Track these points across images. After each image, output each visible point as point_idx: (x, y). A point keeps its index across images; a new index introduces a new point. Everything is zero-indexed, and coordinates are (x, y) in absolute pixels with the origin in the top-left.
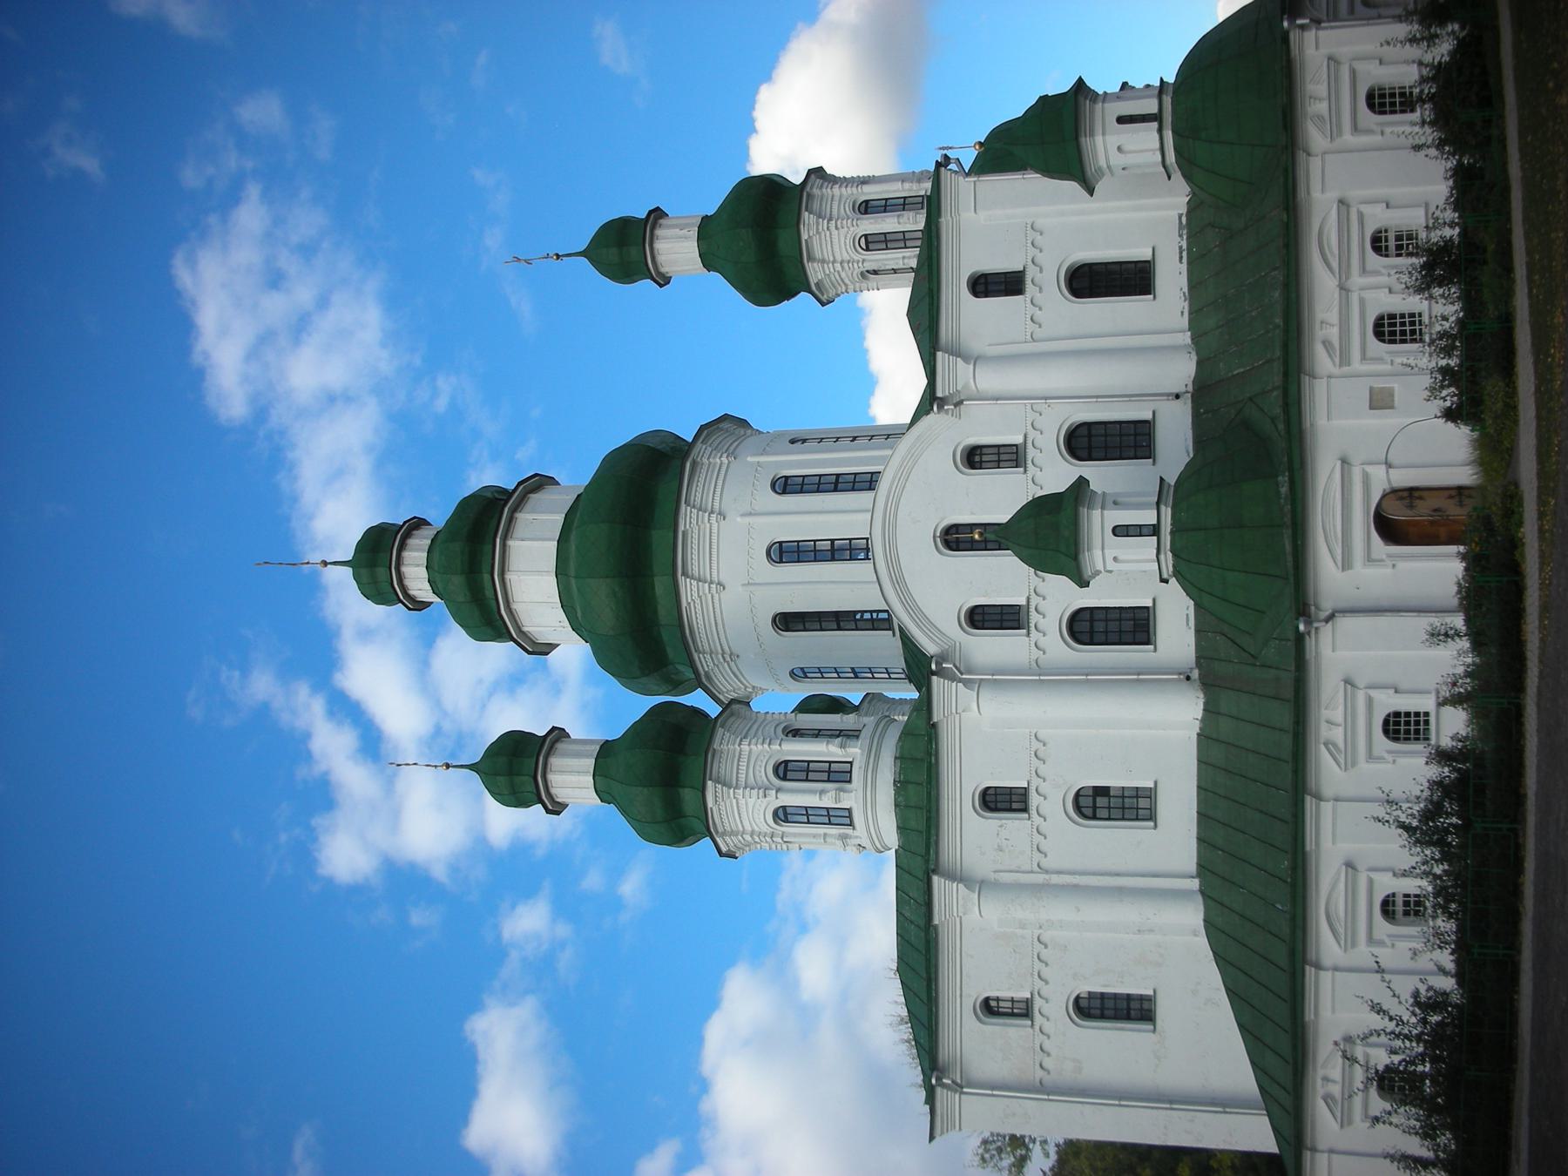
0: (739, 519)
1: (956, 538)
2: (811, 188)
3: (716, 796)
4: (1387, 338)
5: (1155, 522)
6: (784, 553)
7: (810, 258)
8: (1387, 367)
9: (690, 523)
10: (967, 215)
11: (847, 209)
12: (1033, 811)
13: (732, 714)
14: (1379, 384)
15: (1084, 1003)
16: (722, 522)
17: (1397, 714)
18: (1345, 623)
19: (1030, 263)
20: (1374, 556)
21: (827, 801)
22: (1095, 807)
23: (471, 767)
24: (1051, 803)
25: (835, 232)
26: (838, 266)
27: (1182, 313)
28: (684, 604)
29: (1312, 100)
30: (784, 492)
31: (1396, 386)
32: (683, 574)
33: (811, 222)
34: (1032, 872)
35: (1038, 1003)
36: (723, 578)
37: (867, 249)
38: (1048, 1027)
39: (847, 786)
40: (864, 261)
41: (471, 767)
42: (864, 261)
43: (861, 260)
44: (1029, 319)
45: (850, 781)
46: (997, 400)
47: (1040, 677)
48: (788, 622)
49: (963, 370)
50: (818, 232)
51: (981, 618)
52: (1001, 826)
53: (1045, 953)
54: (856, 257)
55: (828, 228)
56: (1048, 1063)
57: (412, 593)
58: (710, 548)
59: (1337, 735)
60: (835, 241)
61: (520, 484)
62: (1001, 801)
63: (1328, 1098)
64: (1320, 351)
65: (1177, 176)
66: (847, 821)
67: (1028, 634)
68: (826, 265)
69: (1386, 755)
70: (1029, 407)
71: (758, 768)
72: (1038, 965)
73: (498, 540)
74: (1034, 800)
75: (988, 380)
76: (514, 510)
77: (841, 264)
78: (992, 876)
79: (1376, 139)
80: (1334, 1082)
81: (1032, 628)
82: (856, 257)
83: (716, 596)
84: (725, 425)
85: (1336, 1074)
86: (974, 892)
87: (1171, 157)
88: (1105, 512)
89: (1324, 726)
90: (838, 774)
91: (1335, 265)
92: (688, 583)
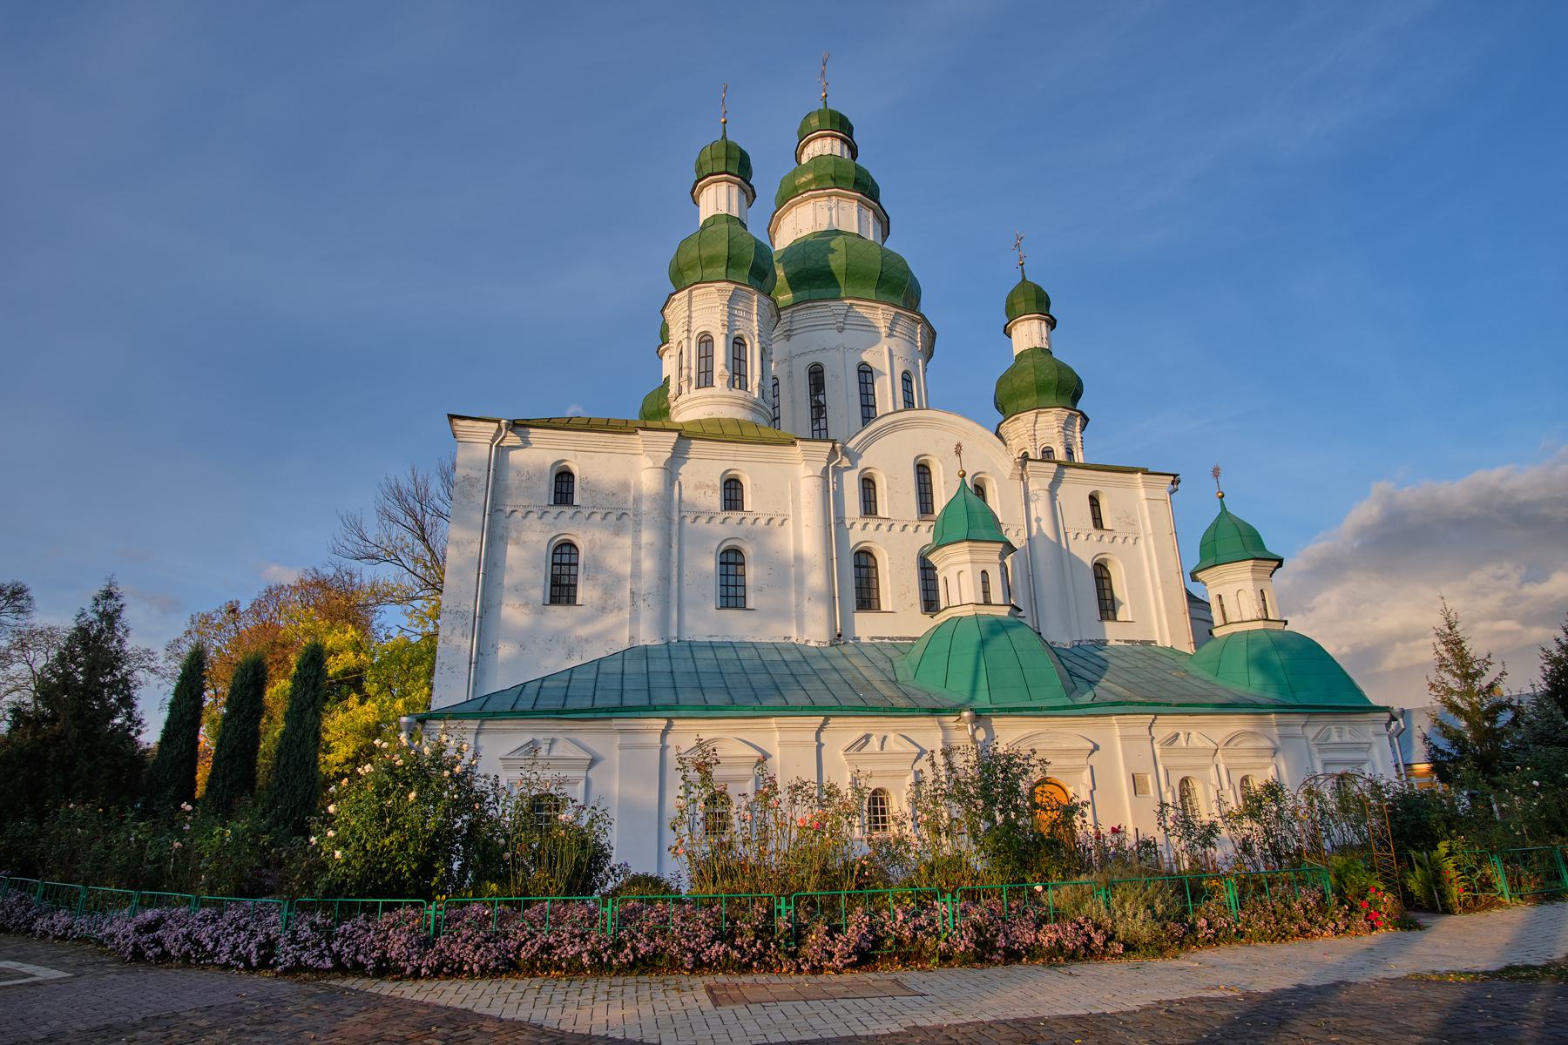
5: (993, 603)
7: (1037, 413)
12: (726, 514)
13: (772, 316)
15: (566, 549)
22: (727, 563)
23: (724, 137)
29: (1339, 730)
30: (903, 379)
34: (680, 512)
35: (569, 511)
36: (845, 332)
37: (1043, 452)
38: (549, 518)
41: (724, 137)
46: (1026, 505)
47: (834, 524)
51: (868, 484)
53: (613, 517)
56: (518, 515)
57: (811, 144)
61: (888, 218)
62: (732, 492)
63: (533, 747)
66: (702, 383)
73: (859, 195)
80: (549, 751)
85: (572, 752)
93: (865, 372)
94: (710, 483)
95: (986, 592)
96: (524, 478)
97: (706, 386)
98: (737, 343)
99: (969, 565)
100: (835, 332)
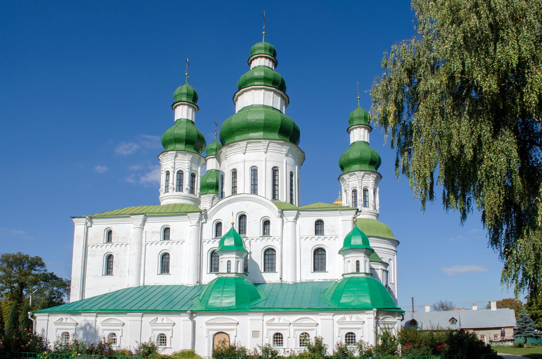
0: (265, 157)
1: (242, 217)
4: (275, 336)
5: (231, 272)
6: (254, 171)
8: (265, 335)
10: (341, 218)
14: (261, 333)
17: (166, 337)
18: (190, 323)
19: (325, 237)
20: (210, 332)
21: (170, 185)
24: (165, 247)
25: (358, 181)
28: (239, 143)
31: (259, 338)
32: (248, 142)
36: (246, 153)
45: (177, 191)
47: (201, 243)
48: (234, 173)
49: (292, 218)
51: (219, 225)
54: (350, 188)
55: (359, 179)
58: (256, 150)
59: (159, 321)
60: (355, 182)
64: (271, 317)
65: (342, 277)
67: (213, 239)
69: (153, 334)
70: (280, 237)
72: (120, 244)
74: (166, 242)
75: (288, 226)
76: (274, 91)
79: (336, 334)
81: (215, 240)
82: (350, 188)
83: (242, 152)
84: (300, 153)
86: (140, 226)
87: (346, 276)
89: (162, 318)
90: (180, 187)
91: (298, 322)
93: (254, 170)
94: (158, 231)
95: (229, 267)
96: (96, 235)
99: (235, 258)
100: (242, 154)
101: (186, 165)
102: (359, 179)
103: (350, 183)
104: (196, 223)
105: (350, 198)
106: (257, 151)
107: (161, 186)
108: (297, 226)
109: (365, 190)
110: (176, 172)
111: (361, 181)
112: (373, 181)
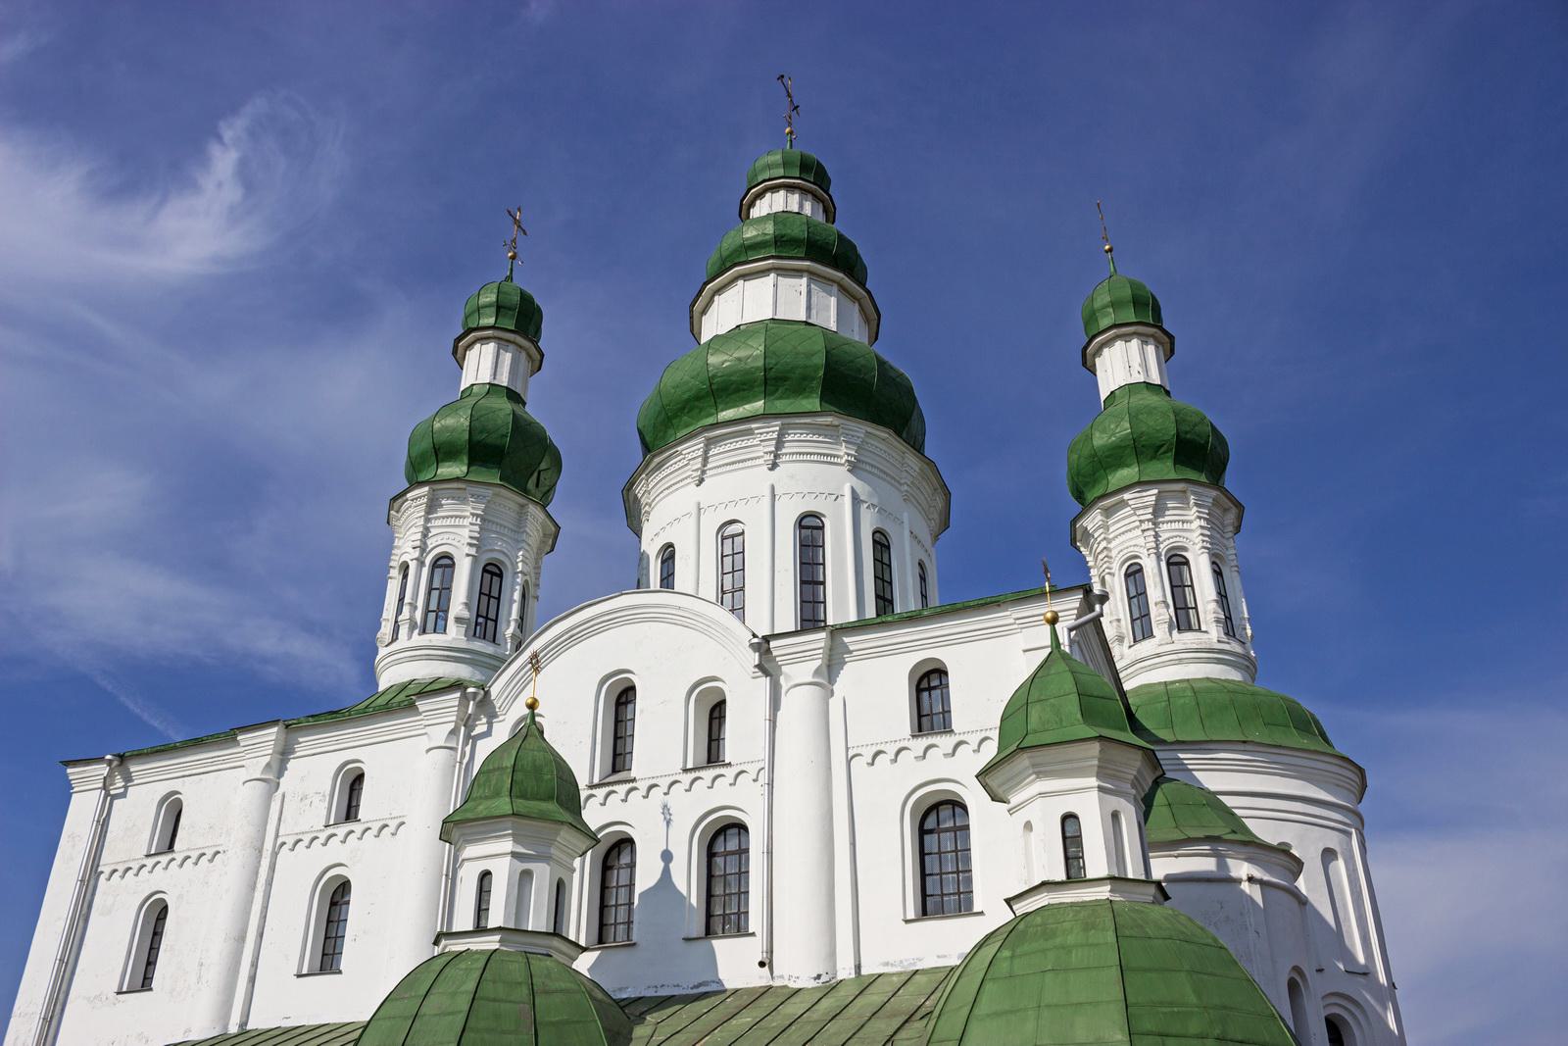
0: (769, 483)
2: (1194, 493)
3: (416, 499)
9: (761, 434)
11: (1175, 540)
16: (765, 468)
26: (1104, 544)
27: (887, 964)
28: (679, 449)
33: (1146, 499)
36: (707, 481)
37: (1127, 575)
39: (416, 631)
40: (1112, 574)
42: (1112, 574)
43: (1112, 571)
44: (879, 748)
50: (1135, 509)
52: (324, 796)
54: (1115, 566)
58: (739, 462)
60: (1129, 535)
68: (1101, 530)
71: (446, 536)
77: (1105, 548)
78: (278, 795)
82: (1115, 566)
88: (509, 858)
92: (699, 446)
97: (435, 632)
98: (441, 566)
100: (693, 485)
101: (466, 533)
102: (1142, 518)
103: (1111, 546)
104: (447, 739)
105: (1119, 604)
106: (741, 465)
107: (383, 624)
108: (835, 704)
109: (1176, 562)
110: (428, 561)
111: (1151, 525)
112: (1203, 523)
